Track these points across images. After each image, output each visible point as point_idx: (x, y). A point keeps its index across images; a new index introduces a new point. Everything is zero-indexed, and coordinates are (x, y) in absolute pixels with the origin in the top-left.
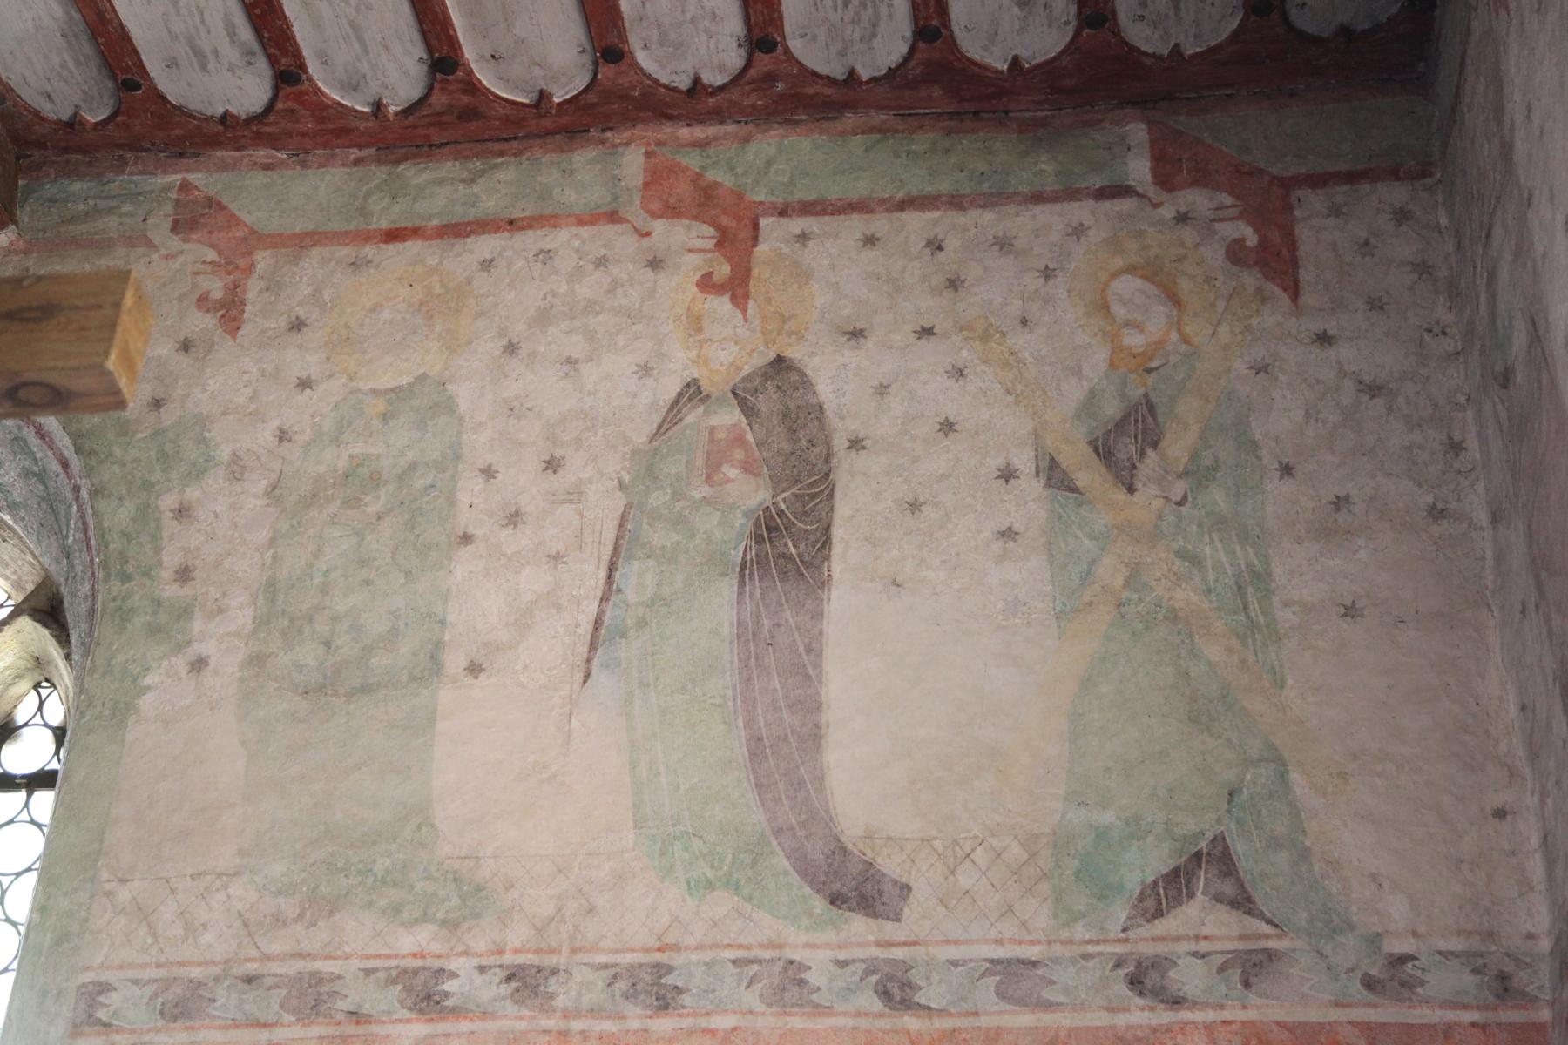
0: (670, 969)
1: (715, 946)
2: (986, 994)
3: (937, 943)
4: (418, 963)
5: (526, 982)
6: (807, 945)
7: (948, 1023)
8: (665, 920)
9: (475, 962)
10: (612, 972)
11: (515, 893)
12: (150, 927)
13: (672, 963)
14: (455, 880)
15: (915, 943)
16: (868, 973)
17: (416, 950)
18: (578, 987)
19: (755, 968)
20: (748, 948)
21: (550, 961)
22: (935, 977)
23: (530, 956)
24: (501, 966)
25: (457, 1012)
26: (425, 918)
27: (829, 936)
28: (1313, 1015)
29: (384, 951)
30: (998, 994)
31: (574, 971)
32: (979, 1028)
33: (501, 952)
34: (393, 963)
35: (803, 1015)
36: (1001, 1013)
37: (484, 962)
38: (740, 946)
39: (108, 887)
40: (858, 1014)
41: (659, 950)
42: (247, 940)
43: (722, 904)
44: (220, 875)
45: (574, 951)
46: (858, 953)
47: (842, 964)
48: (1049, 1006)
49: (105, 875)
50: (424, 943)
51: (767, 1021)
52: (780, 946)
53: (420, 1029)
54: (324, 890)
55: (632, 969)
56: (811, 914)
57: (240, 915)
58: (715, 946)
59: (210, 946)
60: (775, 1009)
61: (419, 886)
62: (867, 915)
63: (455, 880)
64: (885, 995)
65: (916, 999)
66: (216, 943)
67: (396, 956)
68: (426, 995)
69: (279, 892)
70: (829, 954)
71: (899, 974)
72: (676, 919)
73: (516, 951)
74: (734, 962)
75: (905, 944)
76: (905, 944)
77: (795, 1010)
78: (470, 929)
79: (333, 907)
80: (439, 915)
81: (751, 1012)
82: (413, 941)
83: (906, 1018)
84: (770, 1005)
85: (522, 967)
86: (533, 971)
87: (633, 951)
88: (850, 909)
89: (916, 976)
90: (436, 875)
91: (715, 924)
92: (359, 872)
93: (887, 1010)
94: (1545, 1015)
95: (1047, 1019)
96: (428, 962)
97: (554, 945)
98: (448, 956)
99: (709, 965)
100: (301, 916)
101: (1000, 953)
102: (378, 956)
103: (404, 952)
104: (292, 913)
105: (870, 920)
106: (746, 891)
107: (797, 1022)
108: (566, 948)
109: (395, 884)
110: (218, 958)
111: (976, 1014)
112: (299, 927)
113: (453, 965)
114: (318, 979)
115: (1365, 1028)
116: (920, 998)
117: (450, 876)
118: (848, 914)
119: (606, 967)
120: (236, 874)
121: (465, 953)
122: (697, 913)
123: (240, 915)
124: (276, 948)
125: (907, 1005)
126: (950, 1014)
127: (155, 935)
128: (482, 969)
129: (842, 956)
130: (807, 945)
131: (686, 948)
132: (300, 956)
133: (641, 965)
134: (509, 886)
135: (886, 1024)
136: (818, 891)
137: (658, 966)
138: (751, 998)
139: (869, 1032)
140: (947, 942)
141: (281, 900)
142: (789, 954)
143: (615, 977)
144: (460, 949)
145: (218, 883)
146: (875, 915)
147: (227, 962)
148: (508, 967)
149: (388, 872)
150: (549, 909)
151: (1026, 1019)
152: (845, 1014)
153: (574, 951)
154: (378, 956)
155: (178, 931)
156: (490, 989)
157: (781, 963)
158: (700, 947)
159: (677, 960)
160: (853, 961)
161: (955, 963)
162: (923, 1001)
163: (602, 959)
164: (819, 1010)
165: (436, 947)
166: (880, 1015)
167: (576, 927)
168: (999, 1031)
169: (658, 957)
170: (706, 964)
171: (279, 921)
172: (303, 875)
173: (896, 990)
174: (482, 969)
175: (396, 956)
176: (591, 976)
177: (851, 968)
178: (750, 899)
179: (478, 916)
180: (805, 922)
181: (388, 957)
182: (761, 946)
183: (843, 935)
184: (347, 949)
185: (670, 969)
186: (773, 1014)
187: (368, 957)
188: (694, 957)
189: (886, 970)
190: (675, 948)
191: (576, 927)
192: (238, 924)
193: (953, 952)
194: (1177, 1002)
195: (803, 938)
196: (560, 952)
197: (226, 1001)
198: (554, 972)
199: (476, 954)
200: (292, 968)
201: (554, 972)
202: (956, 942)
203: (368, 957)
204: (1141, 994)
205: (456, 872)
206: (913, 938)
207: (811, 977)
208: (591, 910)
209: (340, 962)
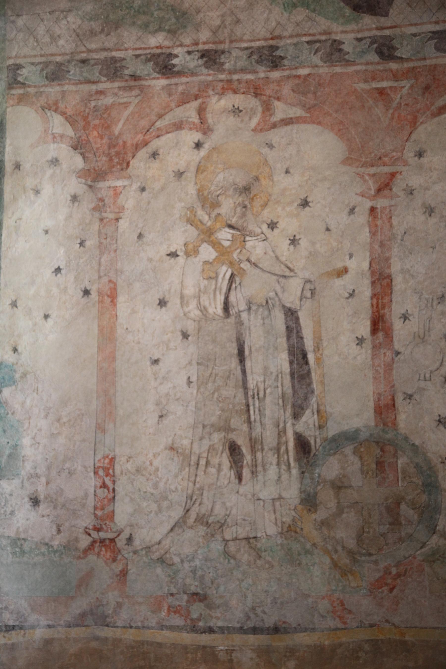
0: (277, 48)
1: (298, 35)
2: (430, 48)
3: (406, 26)
4: (159, 51)
5: (211, 58)
6: (343, 32)
7: (411, 65)
8: (274, 24)
9: (186, 49)
10: (250, 51)
11: (201, 15)
12: (35, 38)
13: (278, 45)
14: (172, 10)
15: (395, 27)
16: (372, 43)
17: (158, 45)
18: (234, 59)
19: (318, 45)
20: (314, 35)
21: (221, 47)
22: (405, 43)
23: (211, 45)
24: (198, 51)
25: (180, 74)
26: (160, 29)
27: (353, 26)
29: (143, 46)
31: (232, 52)
32: (426, 66)
33: (197, 44)
34: (148, 51)
35: (341, 66)
36: (437, 57)
37: (190, 49)
38: (310, 35)
39: (12, 18)
40: (367, 64)
41: (272, 39)
42: (79, 43)
43: (300, 14)
44: (62, 12)
45: (231, 42)
46: (367, 34)
47: (360, 40)
49: (10, 13)
50: (161, 41)
51: (324, 71)
52: (330, 33)
53: (163, 82)
54: (111, 17)
55: (259, 49)
56: (344, 16)
57: (74, 31)
58: (298, 35)
59: (63, 46)
60: (328, 64)
61: (156, 13)
62: (372, 15)
63: (172, 10)
64: (380, 53)
65: (396, 54)
66: (66, 44)
67: (149, 48)
68: (164, 65)
69: (91, 19)
70: (353, 35)
71: (387, 43)
72: (279, 23)
73: (204, 43)
74: (308, 42)
75: (391, 27)
76: (391, 27)
77: (338, 63)
78: (182, 34)
79: (117, 25)
80: (167, 28)
81: (317, 66)
82: (156, 41)
83: (391, 64)
84: (325, 62)
85: (208, 51)
86: (213, 52)
87: (259, 40)
88: (364, 12)
89: (396, 43)
90: (163, 7)
91: (298, 25)
92: (127, 8)
93: (381, 61)
96: (164, 51)
97: (222, 39)
98: (173, 47)
99: (295, 45)
100: (103, 30)
101: (438, 28)
102: (140, 49)
103: (152, 46)
104: (98, 29)
105: (373, 17)
106: (312, 7)
107: (338, 69)
108: (227, 41)
109: (144, 13)
110: (68, 52)
111: (425, 59)
112: (103, 36)
113: (176, 51)
114: (114, 60)
116: (398, 54)
117: (170, 8)
118: (362, 15)
119: (247, 48)
120: (70, 11)
121: (181, 45)
122: (289, 20)
123: (74, 31)
124: (93, 46)
125: (391, 57)
126: (412, 60)
127: (37, 41)
128: (189, 53)
129: (359, 36)
130: (343, 32)
131: (285, 37)
132: (105, 49)
133: (263, 47)
134: (198, 11)
135: (380, 67)
136: (347, 5)
137: (271, 47)
138: (316, 60)
139: (373, 71)
140: (411, 25)
141: (92, 23)
142: (334, 37)
143: (251, 53)
144: (178, 43)
145: (62, 16)
146: (375, 14)
147: (72, 53)
148: (201, 51)
149: (140, 7)
150: (218, 22)
152: (361, 64)
153: (231, 42)
154: (140, 49)
155: (47, 39)
156: (193, 62)
157: (330, 42)
158: (291, 36)
159: (281, 43)
160: (365, 38)
161: (415, 35)
162: (399, 55)
163: (245, 45)
164: (348, 63)
165: (167, 43)
166: (378, 63)
167: (232, 30)
168: (435, 66)
169: (271, 42)
170: (294, 44)
171: (93, 33)
172: (101, 10)
173: (385, 50)
174: (189, 53)
175: (149, 48)
176: (240, 53)
177: (364, 41)
178: (314, 11)
179: (185, 27)
180: (341, 21)
181: (145, 49)
182: (320, 34)
183: (360, 25)
184: (126, 45)
185: (277, 48)
186: (327, 66)
187: (136, 49)
188: (288, 42)
189: (381, 41)
190: (279, 37)
191: (232, 30)
192: (74, 35)
193: (413, 30)
195: (341, 28)
196: (225, 43)
197: (74, 71)
198: (223, 52)
199: (186, 46)
200: (102, 55)
201: (223, 52)
202: (416, 25)
203: (136, 49)
205: (172, 6)
206: (394, 24)
207: (346, 47)
208: (238, 21)
209: (124, 52)
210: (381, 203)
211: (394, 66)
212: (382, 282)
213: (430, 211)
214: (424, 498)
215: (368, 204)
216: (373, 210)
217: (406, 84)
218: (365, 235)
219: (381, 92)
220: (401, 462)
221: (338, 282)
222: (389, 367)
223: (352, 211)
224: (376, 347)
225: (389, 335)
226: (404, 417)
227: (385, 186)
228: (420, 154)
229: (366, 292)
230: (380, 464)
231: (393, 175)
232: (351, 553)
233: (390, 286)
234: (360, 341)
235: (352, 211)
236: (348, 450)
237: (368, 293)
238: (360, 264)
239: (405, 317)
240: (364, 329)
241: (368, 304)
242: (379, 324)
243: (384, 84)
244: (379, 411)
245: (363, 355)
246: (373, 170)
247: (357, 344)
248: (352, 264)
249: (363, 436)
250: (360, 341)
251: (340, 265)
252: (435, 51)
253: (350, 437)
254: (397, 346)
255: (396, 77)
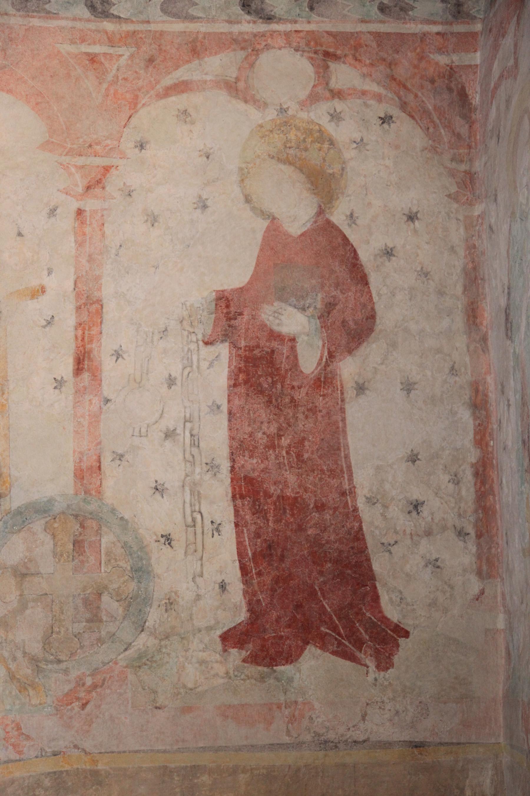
7: (131, 27)
28: (348, 27)
30: (162, 10)
32: (150, 31)
35: (40, 17)
36: (163, 22)
40: (74, 19)
48: (193, 19)
60: (21, 13)
65: (111, 11)
77: (35, 14)
81: (6, 14)
83: (105, 23)
84: (19, 10)
93: (93, 17)
94: (478, 27)
95: (192, 27)
107: (36, 22)
111: (148, 22)
115: (378, 36)
116: (114, 11)
125: (106, 15)
126: (132, 22)
135: (92, 26)
139: (82, 30)
151: (178, 26)
152: (67, 18)
162: (115, 13)
166: (89, 20)
168: (162, 33)
186: (20, 16)
194: (269, 19)
204: (249, 13)
210: (90, 205)
211: (109, 26)
212: (90, 309)
213: (153, 220)
214: (133, 585)
215: (75, 205)
216: (80, 212)
217: (125, 52)
218: (69, 245)
219: (93, 59)
220: (106, 540)
221: (32, 305)
222: (95, 419)
223: (53, 212)
224: (79, 392)
225: (96, 377)
226: (113, 484)
227: (95, 184)
228: (141, 146)
229: (68, 319)
230: (78, 544)
231: (107, 169)
232: (34, 660)
233: (99, 313)
234: (59, 384)
235: (53, 212)
236: (38, 526)
237: (71, 321)
238: (61, 283)
239: (118, 355)
240: (65, 367)
241: (70, 334)
242: (82, 362)
243: (96, 49)
244: (80, 475)
245: (62, 402)
246: (80, 161)
247: (55, 388)
248: (51, 283)
249: (57, 508)
250: (59, 384)
251: (35, 283)
252: (161, 14)
253: (41, 509)
254: (106, 391)
255: (111, 41)
